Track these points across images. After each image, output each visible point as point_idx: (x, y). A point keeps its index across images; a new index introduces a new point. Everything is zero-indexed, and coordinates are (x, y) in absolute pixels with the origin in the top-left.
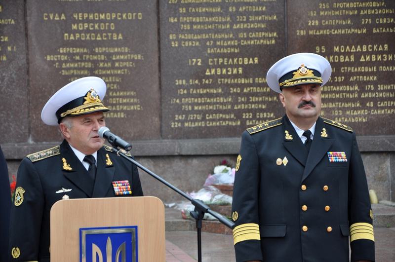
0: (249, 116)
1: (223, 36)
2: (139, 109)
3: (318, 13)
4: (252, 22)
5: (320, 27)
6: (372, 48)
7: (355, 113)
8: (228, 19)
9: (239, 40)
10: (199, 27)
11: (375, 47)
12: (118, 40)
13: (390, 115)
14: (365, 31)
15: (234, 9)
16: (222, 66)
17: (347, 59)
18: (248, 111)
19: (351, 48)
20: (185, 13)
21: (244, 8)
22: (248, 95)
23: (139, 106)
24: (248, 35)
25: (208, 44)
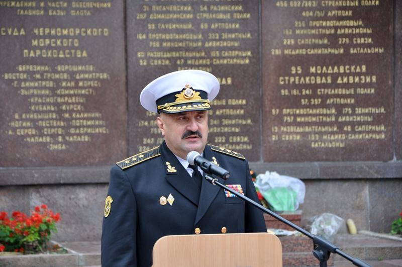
0: (222, 139)
1: (194, 54)
2: (104, 132)
3: (294, 32)
4: (225, 40)
5: (296, 47)
6: (350, 69)
7: (332, 138)
8: (200, 36)
9: (211, 59)
10: (169, 44)
11: (353, 68)
12: (81, 59)
13: (368, 140)
14: (342, 51)
15: (206, 26)
17: (324, 81)
18: (221, 134)
19: (327, 69)
20: (154, 30)
21: (216, 25)
23: (104, 128)
24: (220, 53)
25: (178, 62)
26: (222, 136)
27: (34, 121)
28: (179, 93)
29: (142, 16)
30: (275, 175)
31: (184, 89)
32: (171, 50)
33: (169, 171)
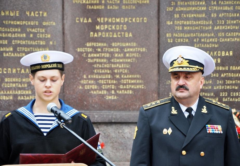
0: (225, 94)
1: (206, 35)
2: (143, 88)
9: (219, 38)
23: (143, 85)
24: (225, 34)
25: (195, 40)
26: (225, 92)
28: (175, 60)
31: (178, 58)
33: (172, 112)
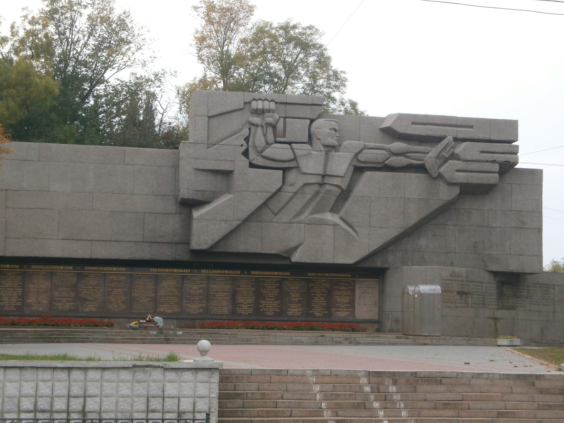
5: (163, 293)
16: (143, 300)
22: (148, 306)
27: (113, 306)
29: (134, 287)
30: (157, 317)
32: (139, 293)
